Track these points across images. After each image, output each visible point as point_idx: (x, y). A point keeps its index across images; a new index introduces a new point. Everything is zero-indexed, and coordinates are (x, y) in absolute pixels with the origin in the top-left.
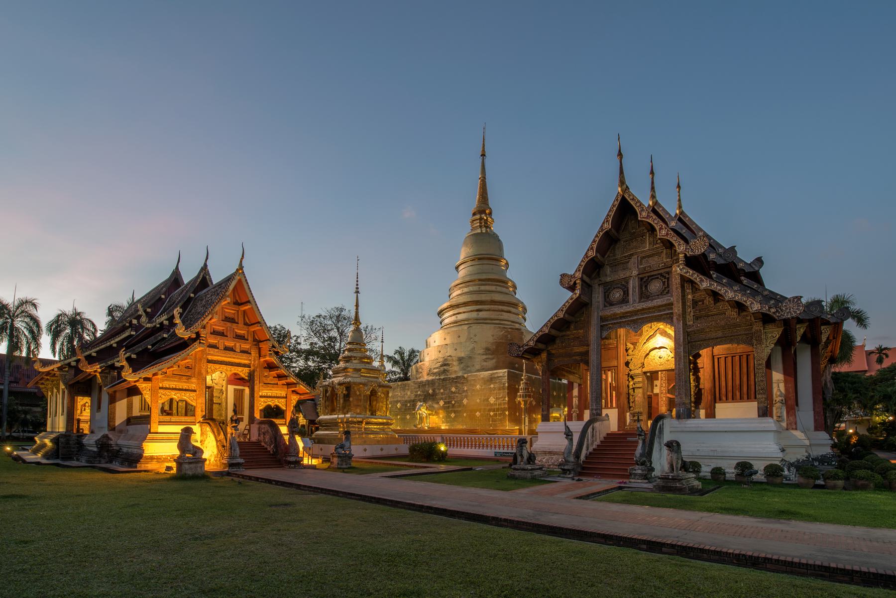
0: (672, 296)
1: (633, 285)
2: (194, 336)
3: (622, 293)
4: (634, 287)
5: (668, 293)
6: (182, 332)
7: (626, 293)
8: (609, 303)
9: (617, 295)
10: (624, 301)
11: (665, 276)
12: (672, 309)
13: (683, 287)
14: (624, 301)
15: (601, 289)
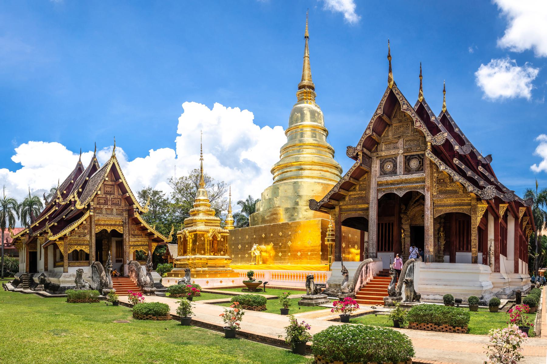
0: (424, 173)
1: (400, 160)
2: (86, 207)
3: (392, 166)
4: (400, 162)
5: (422, 170)
6: (79, 206)
7: (395, 166)
8: (383, 173)
9: (389, 167)
10: (394, 172)
11: (421, 158)
12: (424, 182)
13: (431, 167)
14: (394, 172)
15: (378, 162)
